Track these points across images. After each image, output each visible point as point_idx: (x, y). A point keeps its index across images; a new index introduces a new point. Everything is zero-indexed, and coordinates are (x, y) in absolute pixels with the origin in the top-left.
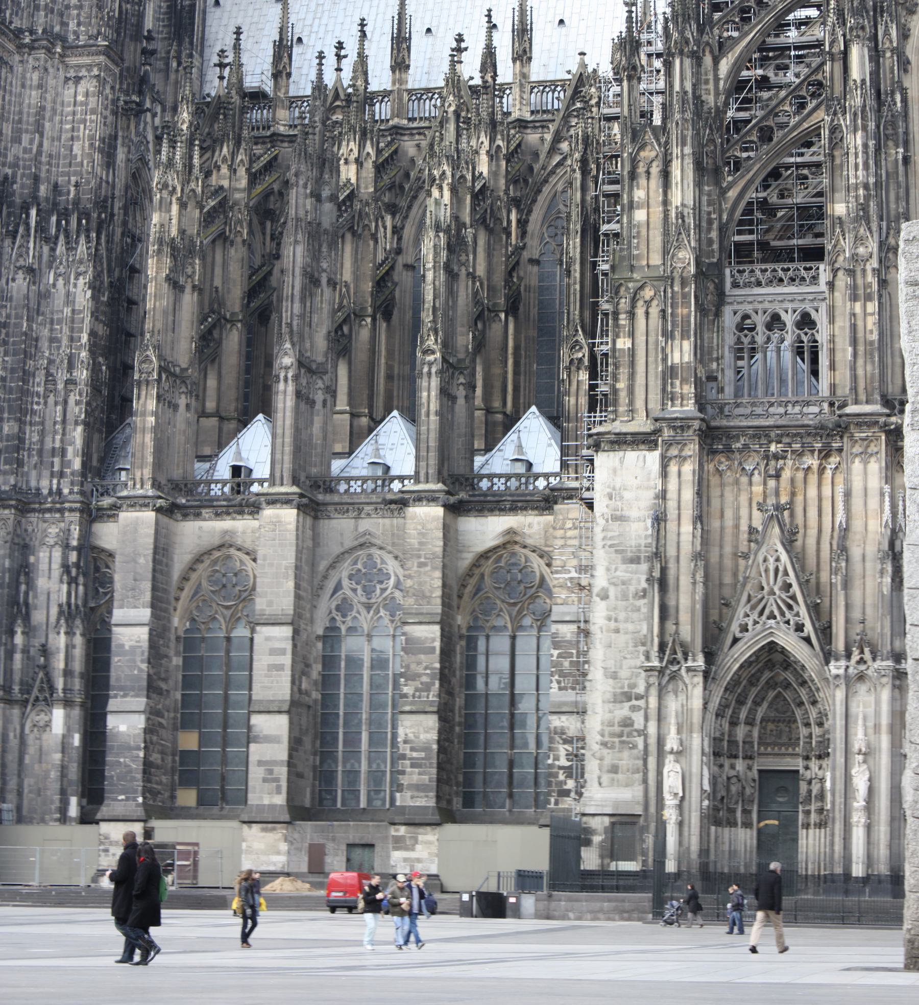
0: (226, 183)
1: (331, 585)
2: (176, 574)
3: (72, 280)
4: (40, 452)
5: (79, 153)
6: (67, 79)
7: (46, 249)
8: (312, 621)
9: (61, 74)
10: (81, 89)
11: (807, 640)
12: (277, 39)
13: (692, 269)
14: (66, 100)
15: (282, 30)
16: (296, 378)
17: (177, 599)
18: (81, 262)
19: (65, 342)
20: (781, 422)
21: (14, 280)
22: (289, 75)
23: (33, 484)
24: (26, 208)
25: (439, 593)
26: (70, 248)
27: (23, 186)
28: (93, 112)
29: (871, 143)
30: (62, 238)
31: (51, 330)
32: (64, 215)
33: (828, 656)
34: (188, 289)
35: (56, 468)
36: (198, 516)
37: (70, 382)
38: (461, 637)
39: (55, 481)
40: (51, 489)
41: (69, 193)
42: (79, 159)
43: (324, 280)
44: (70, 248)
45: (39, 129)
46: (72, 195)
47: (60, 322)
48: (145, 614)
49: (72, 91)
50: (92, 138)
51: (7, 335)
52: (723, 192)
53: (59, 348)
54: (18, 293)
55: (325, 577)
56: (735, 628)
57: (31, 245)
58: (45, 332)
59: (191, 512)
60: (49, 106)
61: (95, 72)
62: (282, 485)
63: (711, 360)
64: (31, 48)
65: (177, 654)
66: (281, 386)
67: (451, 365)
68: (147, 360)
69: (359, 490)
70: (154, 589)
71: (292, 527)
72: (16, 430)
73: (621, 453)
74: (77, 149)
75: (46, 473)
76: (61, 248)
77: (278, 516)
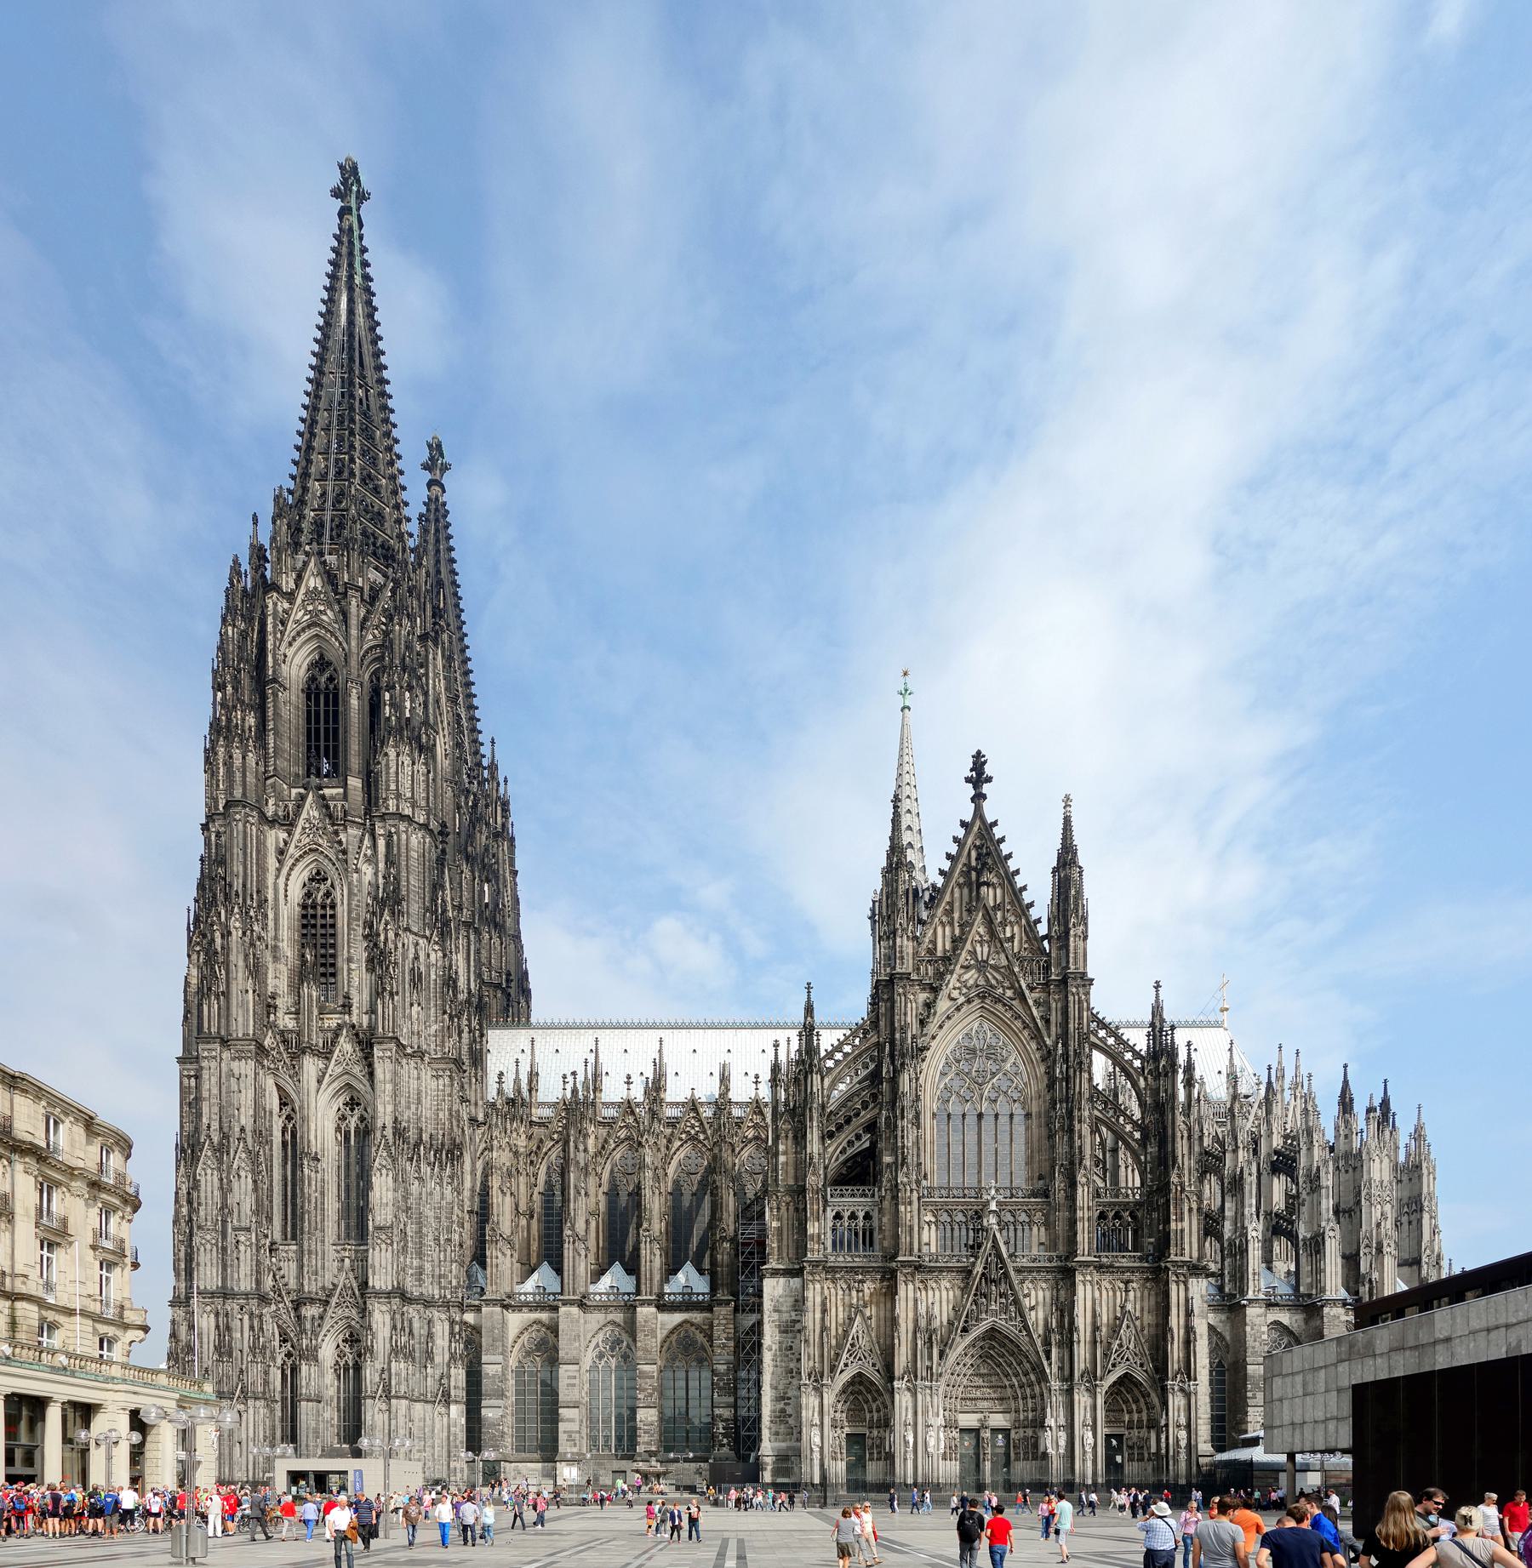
33: (891, 1379)
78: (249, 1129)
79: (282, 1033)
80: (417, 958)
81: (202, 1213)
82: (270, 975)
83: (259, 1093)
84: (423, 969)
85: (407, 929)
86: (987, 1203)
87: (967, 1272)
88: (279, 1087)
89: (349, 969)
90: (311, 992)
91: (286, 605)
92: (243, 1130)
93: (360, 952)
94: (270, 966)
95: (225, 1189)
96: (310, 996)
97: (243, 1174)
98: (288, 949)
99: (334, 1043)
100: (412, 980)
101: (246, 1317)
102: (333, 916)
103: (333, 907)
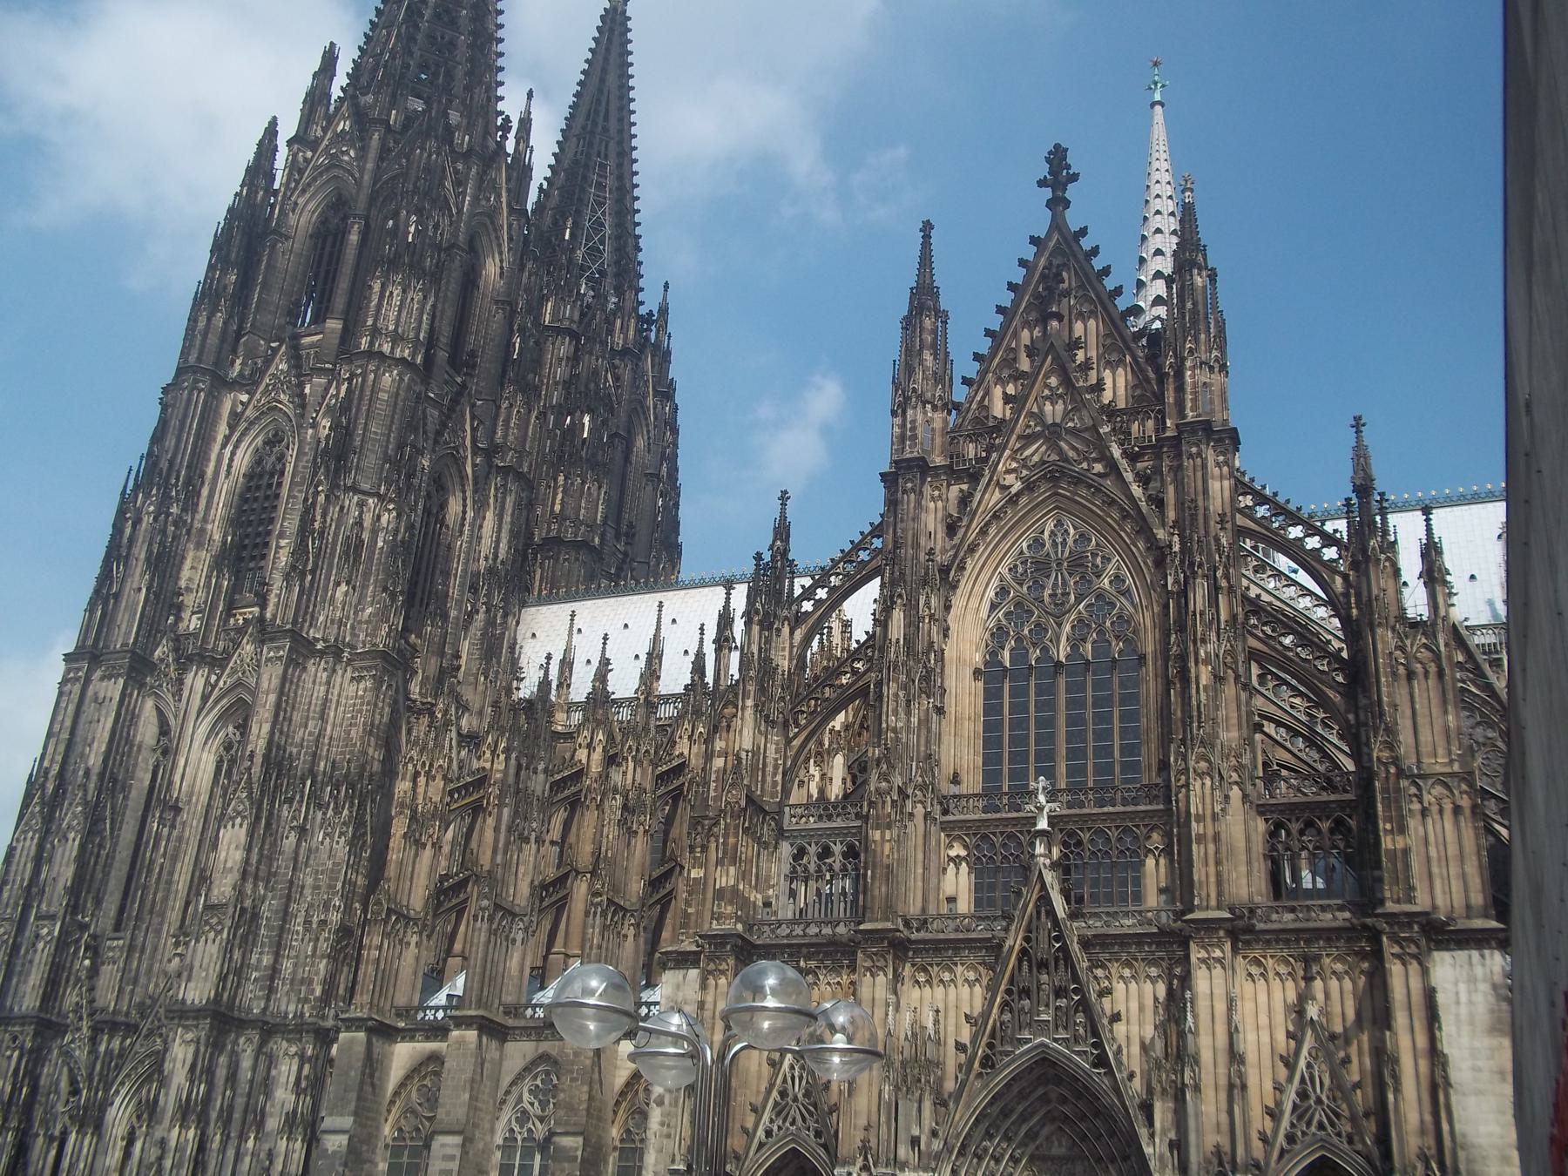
0: (488, 766)
1: (512, 1099)
2: (391, 1087)
4: (292, 981)
7: (319, 814)
8: (492, 1131)
9: (349, 675)
10: (362, 686)
11: (825, 1146)
13: (743, 803)
16: (491, 919)
17: (389, 1111)
18: (344, 823)
20: (814, 940)
22: (569, 686)
23: (283, 1008)
25: (584, 1106)
26: (337, 812)
29: (901, 694)
31: (316, 879)
34: (429, 846)
36: (412, 1039)
37: (323, 923)
38: (615, 1149)
44: (337, 812)
45: (323, 717)
48: (347, 1122)
52: (789, 741)
55: (507, 1093)
56: (760, 1133)
58: (309, 881)
59: (409, 1035)
63: (769, 887)
64: (322, 653)
65: (384, 1160)
67: (619, 908)
68: (378, 903)
70: (359, 1099)
71: (473, 1046)
73: (682, 972)
74: (353, 734)
75: (294, 999)
76: (330, 812)
78: (95, 771)
80: (359, 523)
82: (188, 564)
83: (126, 719)
84: (366, 536)
85: (355, 489)
86: (1032, 821)
87: (994, 948)
89: (278, 547)
91: (309, 154)
92: (87, 773)
94: (190, 555)
96: (218, 586)
97: (72, 835)
100: (346, 553)
101: (16, 1054)
103: (282, 473)
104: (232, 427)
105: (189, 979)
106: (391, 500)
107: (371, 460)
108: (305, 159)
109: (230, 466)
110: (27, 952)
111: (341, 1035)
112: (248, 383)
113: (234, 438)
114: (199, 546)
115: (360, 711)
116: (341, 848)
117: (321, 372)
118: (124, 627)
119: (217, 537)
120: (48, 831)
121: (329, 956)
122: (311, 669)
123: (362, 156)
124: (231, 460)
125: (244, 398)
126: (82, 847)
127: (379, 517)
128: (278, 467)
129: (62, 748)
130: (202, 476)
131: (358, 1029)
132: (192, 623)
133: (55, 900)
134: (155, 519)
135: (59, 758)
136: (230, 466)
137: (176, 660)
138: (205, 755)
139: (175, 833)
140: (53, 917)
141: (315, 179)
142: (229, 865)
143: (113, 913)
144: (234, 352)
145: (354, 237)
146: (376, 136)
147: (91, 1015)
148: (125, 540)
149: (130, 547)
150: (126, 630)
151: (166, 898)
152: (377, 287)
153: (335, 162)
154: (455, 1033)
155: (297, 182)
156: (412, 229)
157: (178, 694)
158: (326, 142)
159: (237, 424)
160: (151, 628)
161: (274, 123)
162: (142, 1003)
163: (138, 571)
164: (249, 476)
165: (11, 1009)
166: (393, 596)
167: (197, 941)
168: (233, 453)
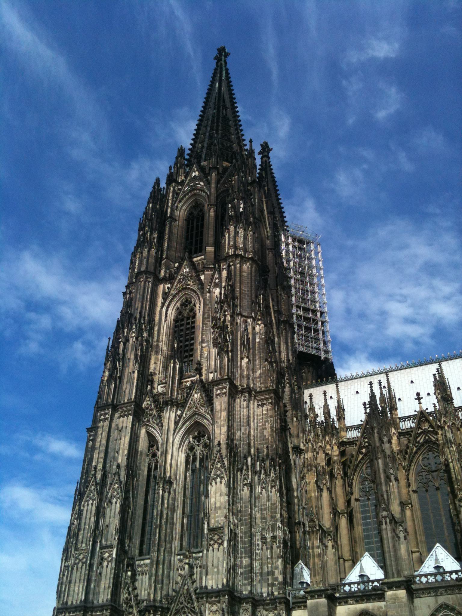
3: (270, 490)
4: (261, 574)
5: (267, 434)
6: (258, 405)
7: (256, 478)
10: (265, 408)
12: (337, 405)
14: (259, 414)
15: (339, 401)
18: (273, 481)
19: (269, 519)
21: (243, 490)
22: (344, 418)
23: (259, 591)
24: (246, 458)
26: (267, 474)
27: (243, 449)
28: (271, 417)
30: (263, 471)
31: (262, 514)
32: (263, 461)
34: (325, 490)
35: (270, 582)
36: (346, 603)
37: (274, 538)
39: (270, 588)
40: (268, 593)
41: (264, 452)
42: (267, 437)
43: (393, 478)
44: (267, 474)
45: (249, 424)
46: (265, 453)
47: (265, 510)
49: (261, 410)
50: (271, 427)
51: (241, 516)
53: (266, 522)
54: (245, 496)
57: (250, 473)
58: (258, 515)
60: (252, 416)
61: (270, 401)
62: (393, 577)
66: (384, 526)
69: (434, 580)
72: (249, 562)
74: (265, 433)
76: (263, 476)
77: (395, 595)
79: (154, 396)
80: (246, 330)
81: (80, 537)
82: (152, 362)
84: (250, 336)
88: (150, 435)
89: (202, 347)
90: (175, 366)
92: (118, 466)
93: (210, 336)
95: (100, 512)
96: (174, 367)
97: (114, 501)
98: (164, 347)
99: (189, 395)
100: (242, 343)
102: (194, 322)
103: (194, 317)
104: (165, 299)
105: (207, 574)
106: (259, 320)
107: (246, 302)
108: (179, 189)
109: (166, 316)
110: (97, 568)
111: (309, 602)
112: (170, 279)
113: (167, 303)
114: (157, 353)
115: (267, 421)
116: (274, 495)
117: (209, 269)
118: (127, 391)
119: (165, 348)
120: (101, 500)
121: (282, 557)
122: (238, 401)
123: (208, 183)
124: (166, 313)
125: (169, 285)
126: (121, 506)
127: (254, 328)
128: (191, 314)
129: (102, 455)
130: (154, 320)
131: (320, 597)
132: (160, 389)
133: (112, 536)
134: (137, 339)
135: (101, 460)
136: (166, 316)
137: (156, 407)
138: (180, 453)
139: (171, 496)
140: (111, 547)
141: (185, 196)
142: (218, 505)
143: (137, 546)
144: (160, 266)
145: (212, 214)
146: (214, 174)
147: (138, 603)
148: (121, 352)
149: (124, 355)
150: (129, 391)
151: (172, 533)
152: (232, 228)
153: (194, 188)
154: (389, 593)
155: (177, 198)
156: (242, 206)
157: (160, 424)
158: (187, 181)
159: (167, 297)
160: (141, 392)
161: (158, 182)
162: (167, 595)
163: (131, 364)
164: (176, 320)
165: (93, 602)
166: (271, 363)
167: (208, 551)
168: (167, 311)
